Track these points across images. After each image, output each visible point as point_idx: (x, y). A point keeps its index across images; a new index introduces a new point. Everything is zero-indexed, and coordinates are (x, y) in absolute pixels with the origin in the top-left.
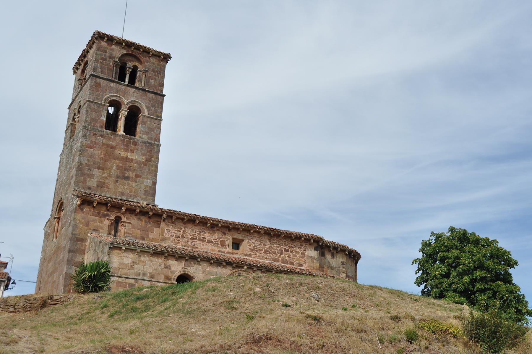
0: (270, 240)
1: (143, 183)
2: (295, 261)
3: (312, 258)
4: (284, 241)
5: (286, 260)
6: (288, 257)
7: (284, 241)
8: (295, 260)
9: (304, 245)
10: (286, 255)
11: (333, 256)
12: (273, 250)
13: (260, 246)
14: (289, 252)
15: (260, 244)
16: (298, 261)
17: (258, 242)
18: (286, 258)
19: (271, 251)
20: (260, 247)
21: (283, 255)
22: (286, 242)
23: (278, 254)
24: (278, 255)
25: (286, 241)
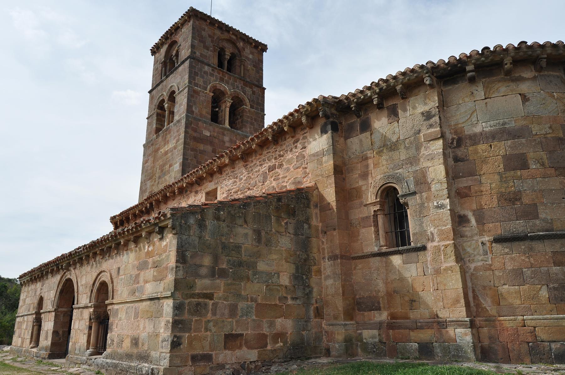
0: (247, 165)
1: (174, 171)
2: (287, 182)
3: (318, 156)
4: (267, 153)
5: (273, 187)
6: (274, 180)
7: (267, 153)
8: (286, 180)
9: (301, 138)
10: (272, 177)
11: (393, 113)
12: (252, 182)
13: (235, 186)
14: (277, 170)
15: (235, 182)
16: (292, 179)
17: (232, 180)
18: (272, 185)
19: (249, 184)
20: (235, 187)
21: (268, 181)
22: (270, 152)
23: (261, 184)
24: (259, 186)
25: (269, 151)
